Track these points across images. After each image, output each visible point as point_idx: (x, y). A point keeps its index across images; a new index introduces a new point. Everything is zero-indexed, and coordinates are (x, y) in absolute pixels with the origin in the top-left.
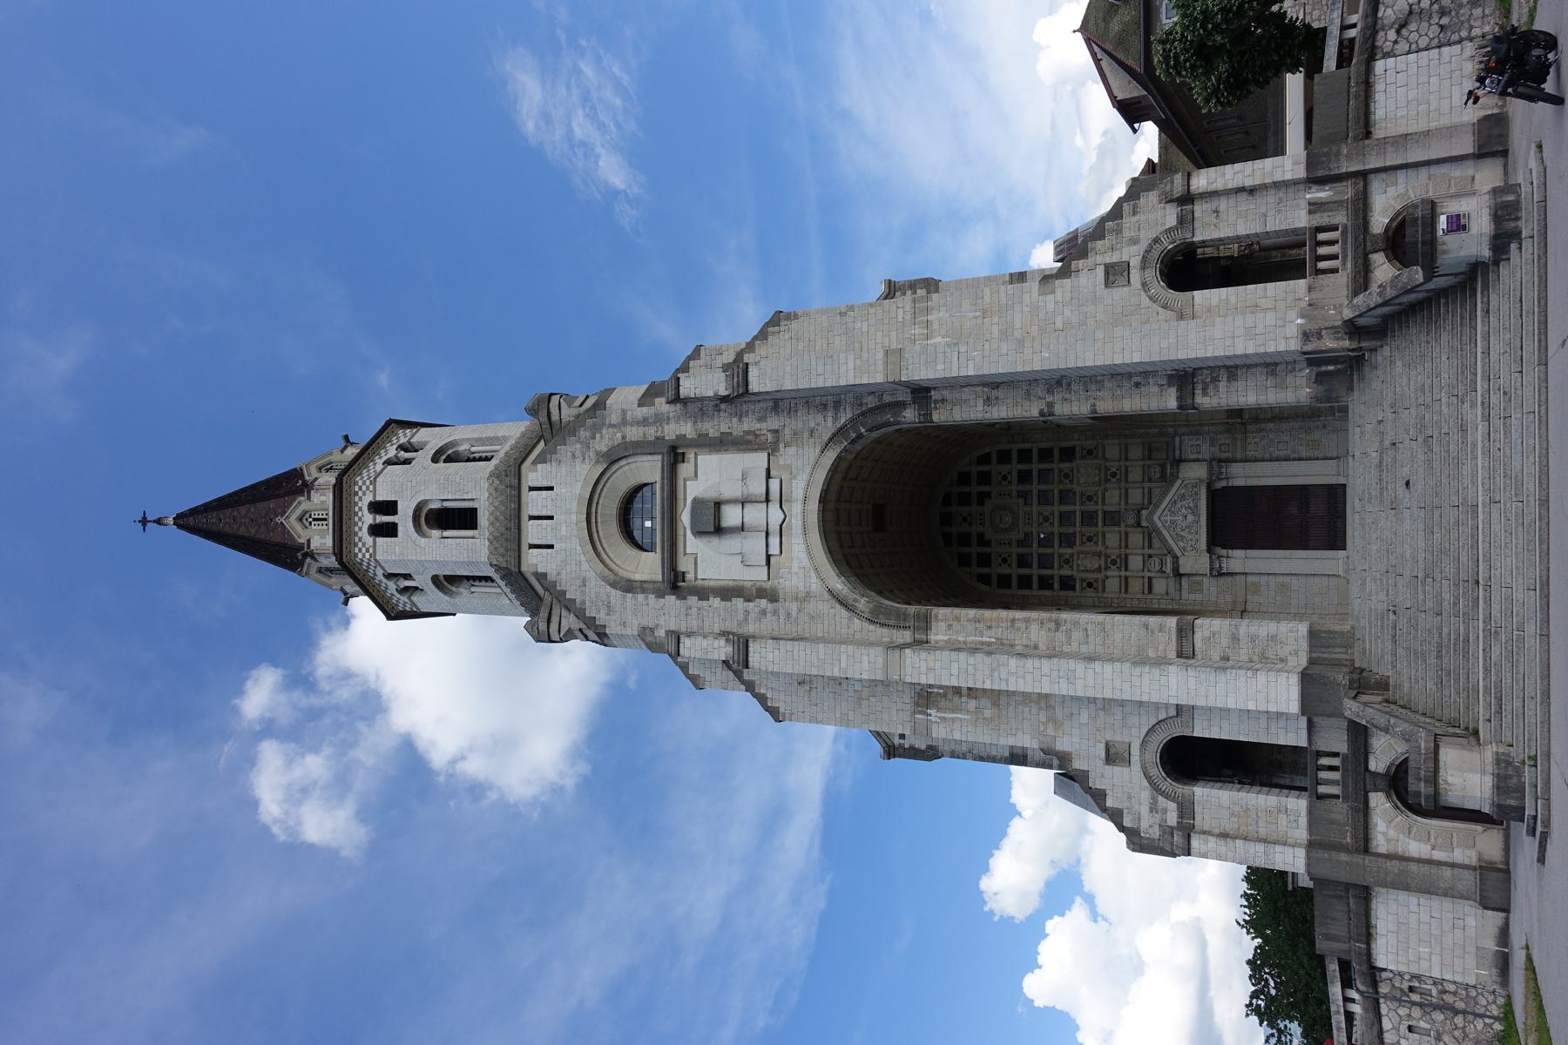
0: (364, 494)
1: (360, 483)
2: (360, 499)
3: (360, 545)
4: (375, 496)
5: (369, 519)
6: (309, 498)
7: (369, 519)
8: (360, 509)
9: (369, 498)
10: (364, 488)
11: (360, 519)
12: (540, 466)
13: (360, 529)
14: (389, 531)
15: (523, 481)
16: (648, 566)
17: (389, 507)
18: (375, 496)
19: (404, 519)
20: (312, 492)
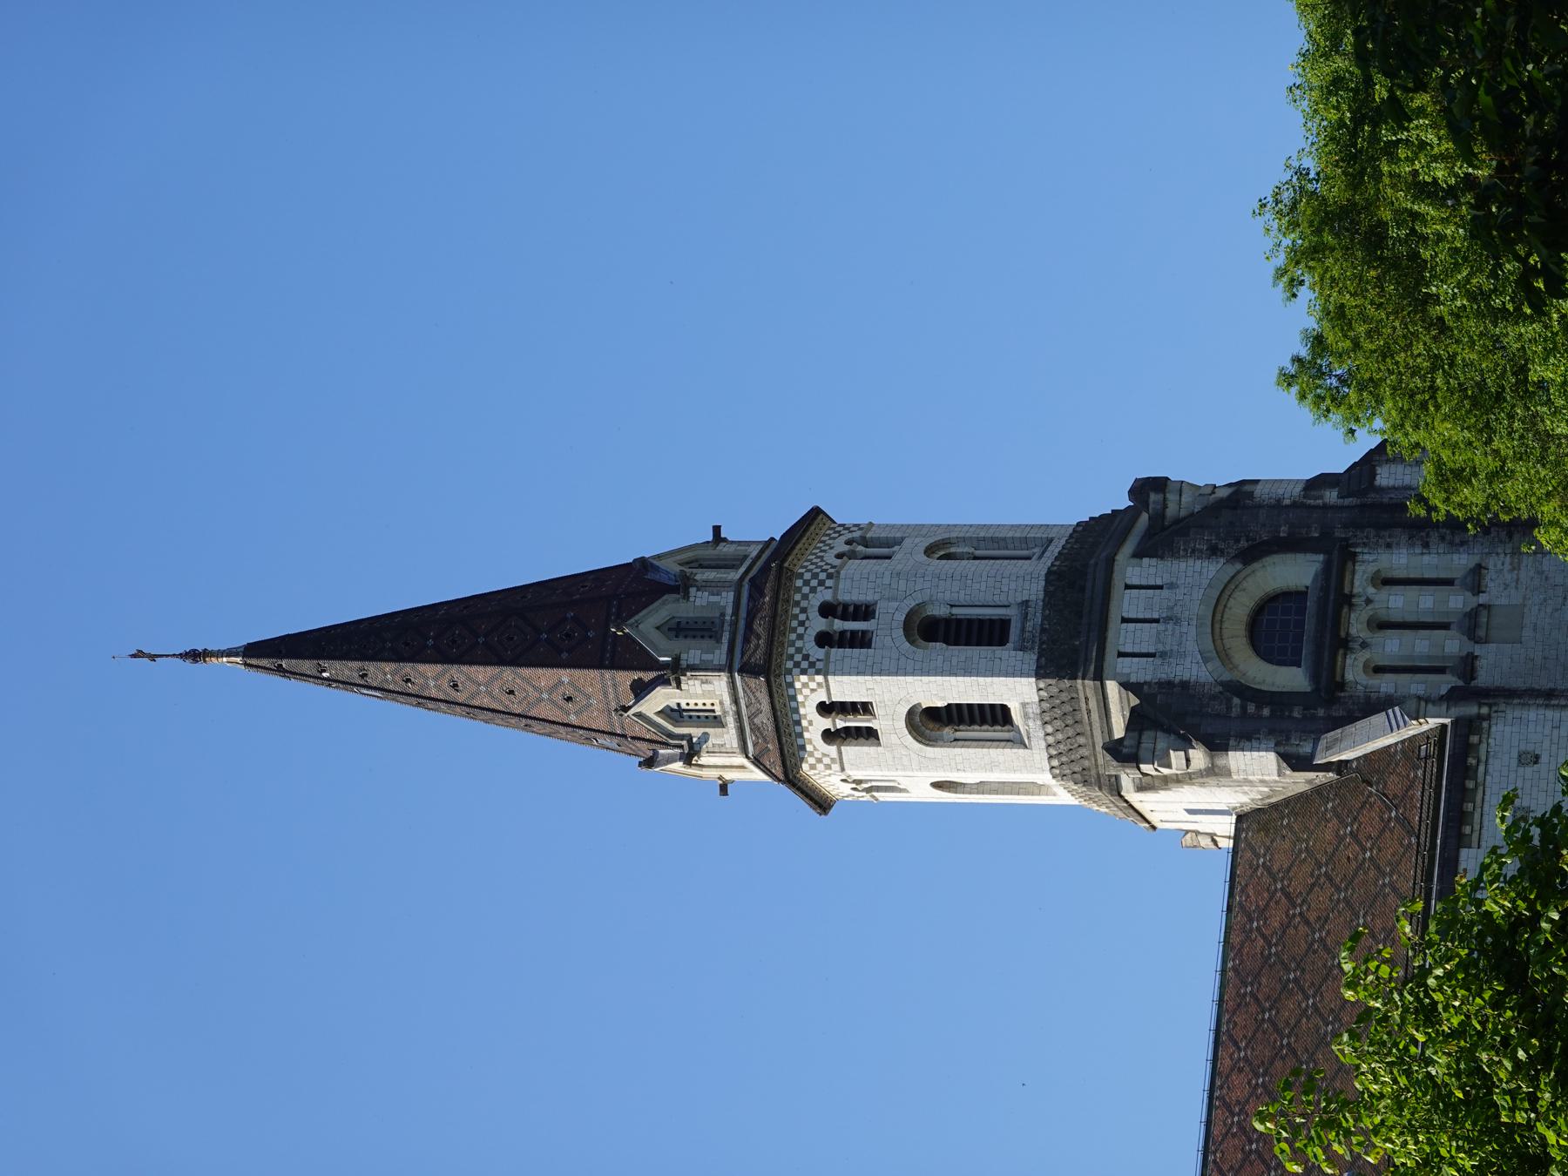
0: (813, 590)
1: (807, 576)
2: (805, 597)
3: (798, 658)
4: (835, 593)
5: (818, 624)
6: (686, 596)
7: (818, 624)
8: (804, 610)
9: (827, 596)
10: (814, 583)
11: (802, 624)
12: (1146, 561)
13: (800, 637)
14: (860, 641)
15: (1117, 577)
16: (1292, 679)
17: (864, 612)
18: (835, 593)
19: (887, 626)
20: (693, 590)
